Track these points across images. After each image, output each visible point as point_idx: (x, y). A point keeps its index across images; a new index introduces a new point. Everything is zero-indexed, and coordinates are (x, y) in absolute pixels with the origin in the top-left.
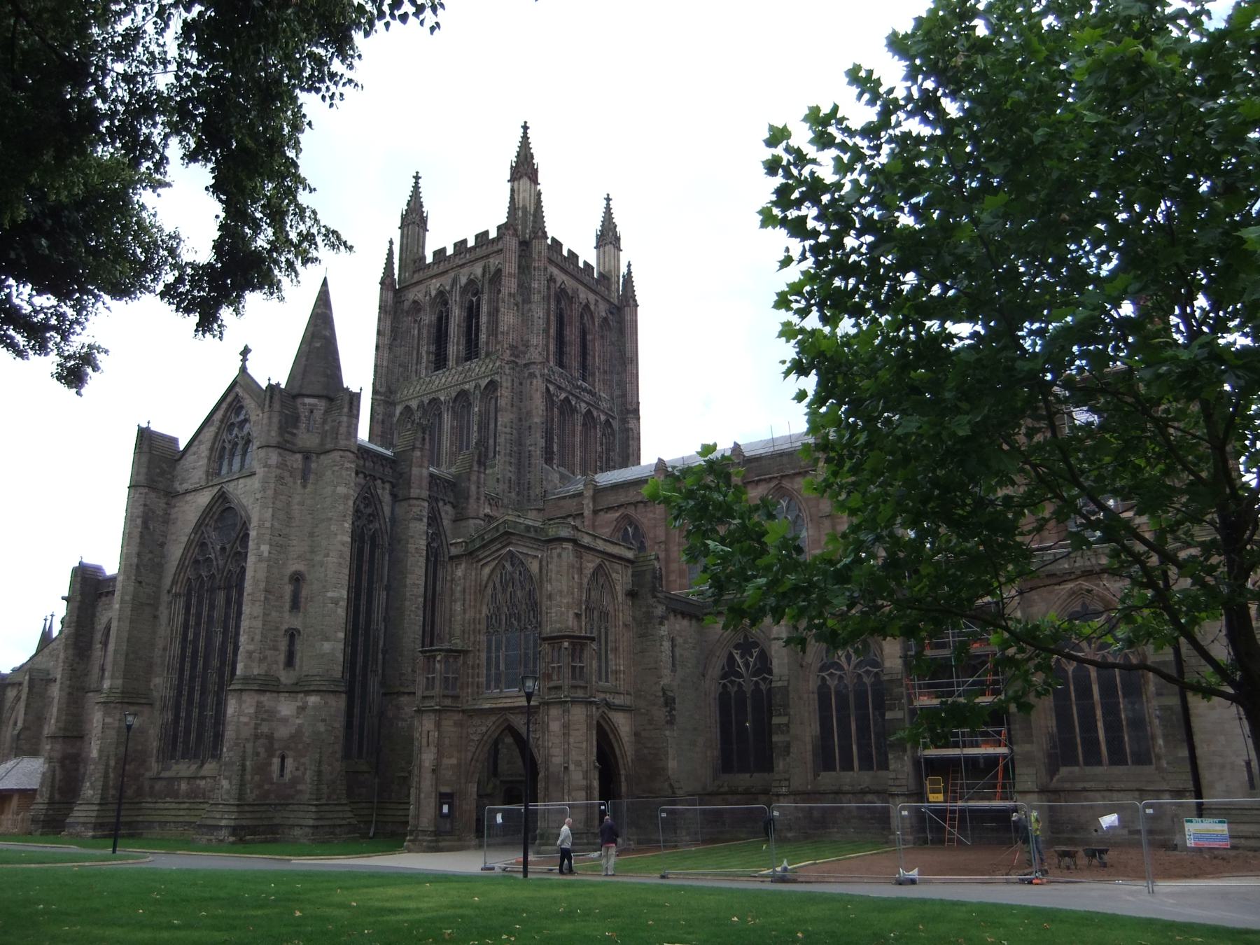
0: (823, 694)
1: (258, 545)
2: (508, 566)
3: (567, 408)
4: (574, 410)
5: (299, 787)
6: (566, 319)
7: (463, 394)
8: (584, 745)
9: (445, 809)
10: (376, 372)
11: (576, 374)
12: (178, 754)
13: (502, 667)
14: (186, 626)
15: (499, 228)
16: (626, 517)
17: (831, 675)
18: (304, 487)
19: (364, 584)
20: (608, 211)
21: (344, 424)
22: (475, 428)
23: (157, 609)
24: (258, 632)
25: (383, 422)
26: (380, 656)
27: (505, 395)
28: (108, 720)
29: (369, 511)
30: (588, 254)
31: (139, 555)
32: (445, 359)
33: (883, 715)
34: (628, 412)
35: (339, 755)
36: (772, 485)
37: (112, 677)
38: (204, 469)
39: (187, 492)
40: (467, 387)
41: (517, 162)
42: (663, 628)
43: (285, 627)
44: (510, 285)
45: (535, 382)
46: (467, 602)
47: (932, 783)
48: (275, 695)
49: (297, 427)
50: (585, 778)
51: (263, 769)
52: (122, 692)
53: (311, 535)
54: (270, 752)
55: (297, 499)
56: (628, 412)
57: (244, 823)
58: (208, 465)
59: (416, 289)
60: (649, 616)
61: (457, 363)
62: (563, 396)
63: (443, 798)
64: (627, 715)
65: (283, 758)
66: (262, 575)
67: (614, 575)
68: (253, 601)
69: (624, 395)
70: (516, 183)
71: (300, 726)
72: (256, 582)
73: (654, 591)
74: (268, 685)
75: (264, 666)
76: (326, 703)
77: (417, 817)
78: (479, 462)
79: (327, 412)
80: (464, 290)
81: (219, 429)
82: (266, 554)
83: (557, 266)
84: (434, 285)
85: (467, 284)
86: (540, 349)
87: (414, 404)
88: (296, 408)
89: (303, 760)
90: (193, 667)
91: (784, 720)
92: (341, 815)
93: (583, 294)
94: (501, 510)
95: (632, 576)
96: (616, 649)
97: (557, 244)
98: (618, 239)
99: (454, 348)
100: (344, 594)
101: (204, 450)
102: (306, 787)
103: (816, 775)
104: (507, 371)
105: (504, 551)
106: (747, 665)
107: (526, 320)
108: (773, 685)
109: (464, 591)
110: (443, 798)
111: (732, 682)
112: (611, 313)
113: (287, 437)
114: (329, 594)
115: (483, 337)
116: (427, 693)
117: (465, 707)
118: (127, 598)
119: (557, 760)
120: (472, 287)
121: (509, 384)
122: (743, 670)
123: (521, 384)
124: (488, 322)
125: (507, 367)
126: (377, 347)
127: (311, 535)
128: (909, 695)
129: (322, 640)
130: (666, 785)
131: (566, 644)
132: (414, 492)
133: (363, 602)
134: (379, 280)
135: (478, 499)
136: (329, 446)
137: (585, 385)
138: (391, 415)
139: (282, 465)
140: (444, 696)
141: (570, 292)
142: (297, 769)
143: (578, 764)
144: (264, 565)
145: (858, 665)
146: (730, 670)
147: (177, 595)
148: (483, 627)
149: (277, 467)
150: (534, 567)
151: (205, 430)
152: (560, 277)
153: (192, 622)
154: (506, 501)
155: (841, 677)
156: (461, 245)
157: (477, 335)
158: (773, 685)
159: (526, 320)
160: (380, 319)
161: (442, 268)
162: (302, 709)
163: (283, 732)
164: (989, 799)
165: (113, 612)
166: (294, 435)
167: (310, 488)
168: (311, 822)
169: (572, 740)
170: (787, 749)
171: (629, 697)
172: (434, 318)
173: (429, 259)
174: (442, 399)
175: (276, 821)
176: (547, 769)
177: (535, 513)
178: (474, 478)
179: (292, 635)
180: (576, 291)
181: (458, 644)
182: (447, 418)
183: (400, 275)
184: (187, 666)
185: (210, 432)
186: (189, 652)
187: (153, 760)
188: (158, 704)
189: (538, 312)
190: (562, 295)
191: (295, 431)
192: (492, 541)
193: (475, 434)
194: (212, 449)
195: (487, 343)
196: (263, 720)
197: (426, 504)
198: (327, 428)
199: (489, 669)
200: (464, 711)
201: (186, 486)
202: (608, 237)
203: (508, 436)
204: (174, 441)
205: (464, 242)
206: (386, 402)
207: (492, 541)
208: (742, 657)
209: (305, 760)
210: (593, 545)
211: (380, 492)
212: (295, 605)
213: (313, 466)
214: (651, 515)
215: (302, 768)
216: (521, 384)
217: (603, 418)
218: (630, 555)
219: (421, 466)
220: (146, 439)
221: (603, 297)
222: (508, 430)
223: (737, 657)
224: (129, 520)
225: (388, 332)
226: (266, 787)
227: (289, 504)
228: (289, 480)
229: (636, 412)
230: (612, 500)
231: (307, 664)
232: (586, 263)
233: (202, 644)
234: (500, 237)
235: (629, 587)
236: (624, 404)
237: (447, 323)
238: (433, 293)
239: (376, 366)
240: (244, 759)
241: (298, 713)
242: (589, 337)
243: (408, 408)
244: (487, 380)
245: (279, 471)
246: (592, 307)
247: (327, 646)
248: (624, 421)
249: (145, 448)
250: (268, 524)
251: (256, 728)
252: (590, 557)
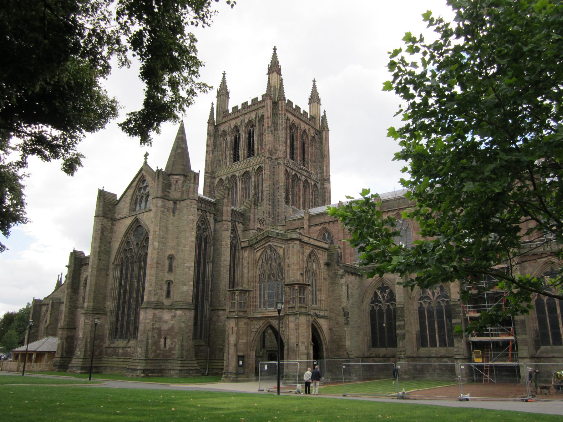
0: (421, 312)
1: (153, 242)
2: (269, 251)
3: (296, 179)
4: (299, 179)
5: (173, 352)
6: (295, 138)
7: (247, 173)
8: (306, 334)
9: (241, 363)
10: (206, 163)
11: (300, 163)
12: (118, 336)
13: (266, 298)
14: (121, 279)
15: (263, 96)
16: (324, 228)
17: (425, 302)
18: (174, 216)
19: (202, 260)
20: (314, 87)
21: (192, 187)
22: (253, 188)
23: (108, 271)
24: (154, 281)
25: (210, 186)
26: (210, 293)
27: (266, 173)
28: (87, 321)
29: (204, 227)
30: (305, 107)
31: (100, 247)
32: (238, 157)
33: (451, 321)
34: (325, 180)
35: (191, 338)
36: (395, 213)
37: (88, 302)
38: (128, 208)
39: (121, 219)
40: (248, 169)
41: (271, 66)
42: (342, 280)
43: (166, 279)
44: (268, 122)
45: (280, 166)
46: (250, 268)
47: (476, 353)
48: (161, 310)
49: (170, 188)
50: (307, 349)
51: (156, 343)
52: (93, 309)
53: (177, 238)
54: (160, 336)
55: (171, 221)
56: (325, 180)
57: (148, 368)
58: (130, 206)
59: (224, 125)
60: (336, 274)
61: (244, 159)
62: (294, 173)
63: (240, 358)
64: (326, 320)
65: (165, 339)
66: (155, 256)
67: (319, 256)
68: (151, 268)
69: (323, 172)
70: (271, 75)
71: (173, 324)
72: (152, 260)
73: (338, 262)
74: (158, 306)
75: (157, 297)
76: (185, 314)
77: (228, 366)
78: (255, 204)
79: (184, 182)
80: (247, 125)
81: (135, 190)
82: (157, 246)
83: (290, 113)
84: (233, 123)
85: (248, 122)
86: (282, 152)
87: (224, 178)
88: (170, 180)
89: (175, 340)
90: (124, 298)
91: (402, 323)
92: (192, 365)
93: (303, 126)
94: (265, 226)
95: (328, 256)
96: (320, 290)
97: (290, 103)
98: (319, 100)
99: (242, 152)
100: (193, 264)
101: (128, 199)
102: (176, 352)
103: (418, 349)
104: (267, 162)
105: (267, 245)
106: (383, 297)
107: (276, 138)
108: (397, 306)
109: (248, 263)
110: (240, 358)
111: (376, 305)
112: (316, 134)
113: (166, 193)
114: (186, 265)
115: (256, 147)
116: (232, 310)
117: (249, 316)
118: (95, 266)
119: (293, 341)
120: (251, 124)
121: (268, 168)
122: (382, 300)
123: (274, 168)
124: (258, 140)
125: (267, 160)
126: (207, 152)
127: (177, 238)
128: (464, 312)
129: (183, 285)
130: (345, 353)
131: (296, 287)
132: (225, 218)
133: (202, 268)
134: (207, 121)
135: (254, 221)
136: (185, 197)
137: (304, 168)
138: (214, 183)
139: (164, 206)
140: (239, 311)
141: (296, 125)
142: (172, 344)
143: (303, 342)
144: (156, 251)
145: (438, 297)
146: (375, 300)
147: (117, 265)
148: (257, 279)
149: (161, 207)
150: (281, 252)
151: (129, 191)
152: (292, 118)
153: (124, 277)
154: (267, 222)
155: (430, 303)
156: (245, 105)
157: (253, 146)
158: (397, 306)
159: (276, 138)
160: (208, 139)
161: (236, 115)
162: (174, 316)
163: (165, 327)
164: (505, 361)
165: (88, 273)
166: (169, 192)
167: (176, 216)
168: (179, 368)
169: (300, 332)
170: (404, 336)
171: (326, 312)
172: (233, 138)
173: (230, 111)
174: (237, 175)
175: (163, 367)
176: (288, 345)
177: (281, 227)
178: (252, 211)
179: (169, 283)
180: (299, 125)
181: (246, 287)
182: (239, 184)
183: (217, 119)
184: (122, 297)
185: (131, 192)
186: (122, 291)
187: (107, 339)
188: (109, 314)
189: (282, 134)
190: (293, 126)
192: (261, 240)
193: (253, 191)
194: (132, 199)
195: (258, 149)
196: (156, 321)
197: (230, 223)
198: (184, 189)
199: (260, 299)
200: (249, 318)
201: (120, 216)
202: (314, 99)
203: (268, 192)
204: (115, 195)
205: (247, 103)
206: (211, 177)
207: (261, 240)
208: (381, 293)
209: (176, 340)
210: (308, 242)
211: (208, 218)
212: (170, 269)
213: (178, 206)
214: (336, 228)
215: (174, 343)
216: (274, 168)
217: (313, 183)
218: (326, 246)
219: (228, 206)
220: (103, 196)
221: (312, 127)
222: (268, 189)
223: (379, 294)
224: (95, 231)
225: (211, 145)
226: (158, 352)
227: (167, 224)
228: (166, 212)
229: (328, 180)
230: (318, 221)
231: (176, 296)
232: (304, 111)
233: (128, 287)
234: (263, 101)
235: (326, 261)
236: (323, 176)
237: (239, 140)
238: (232, 127)
239: (206, 161)
240: (148, 339)
241: (172, 319)
242: (306, 146)
243: (221, 179)
244: (258, 167)
245: (162, 209)
246: (307, 132)
247: (185, 288)
248: (323, 184)
249: (102, 199)
250: (157, 233)
251: (153, 325)
252: (307, 247)
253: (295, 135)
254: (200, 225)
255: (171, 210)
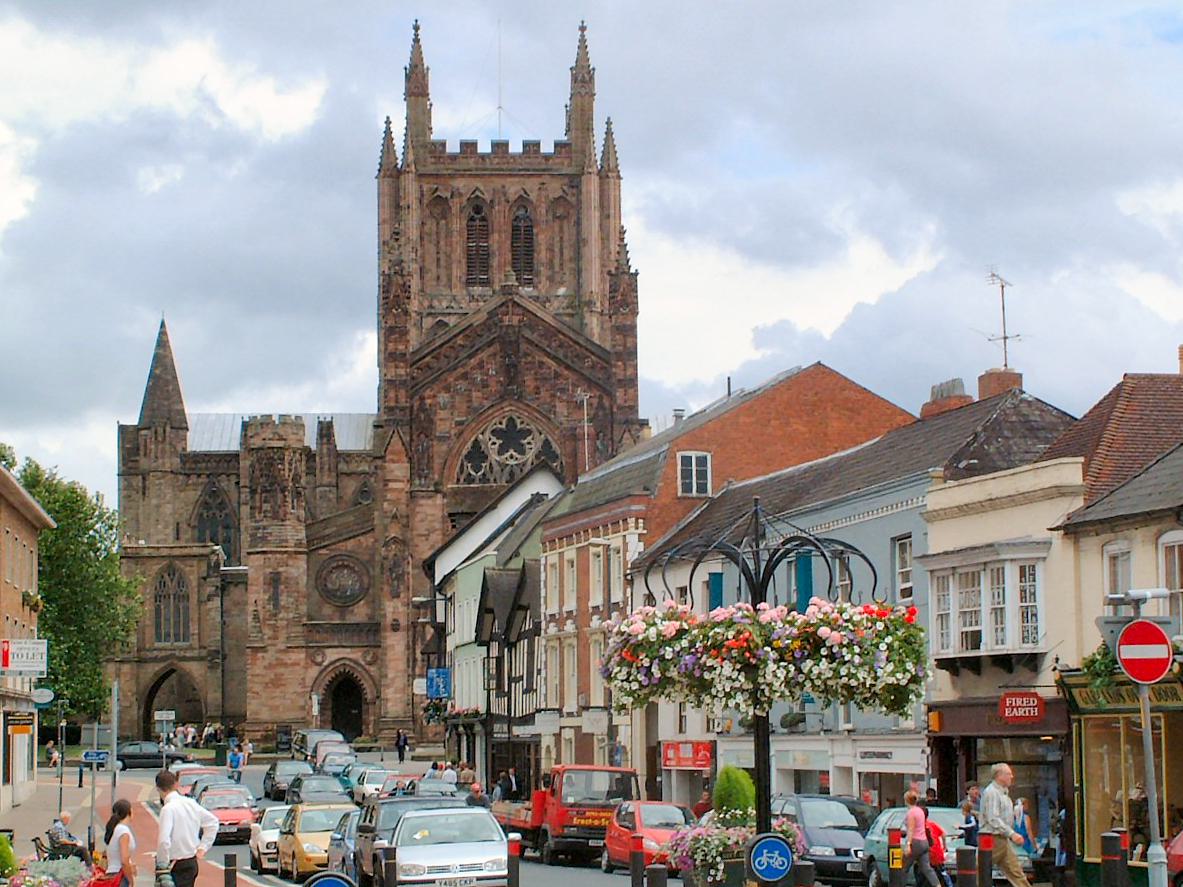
20: (583, 45)
49: (138, 455)
135: (322, 468)
141: (487, 197)
166: (137, 461)
191: (138, 458)
227: (137, 514)
228: (134, 496)
245: (126, 492)
254: (210, 501)
255: (141, 493)
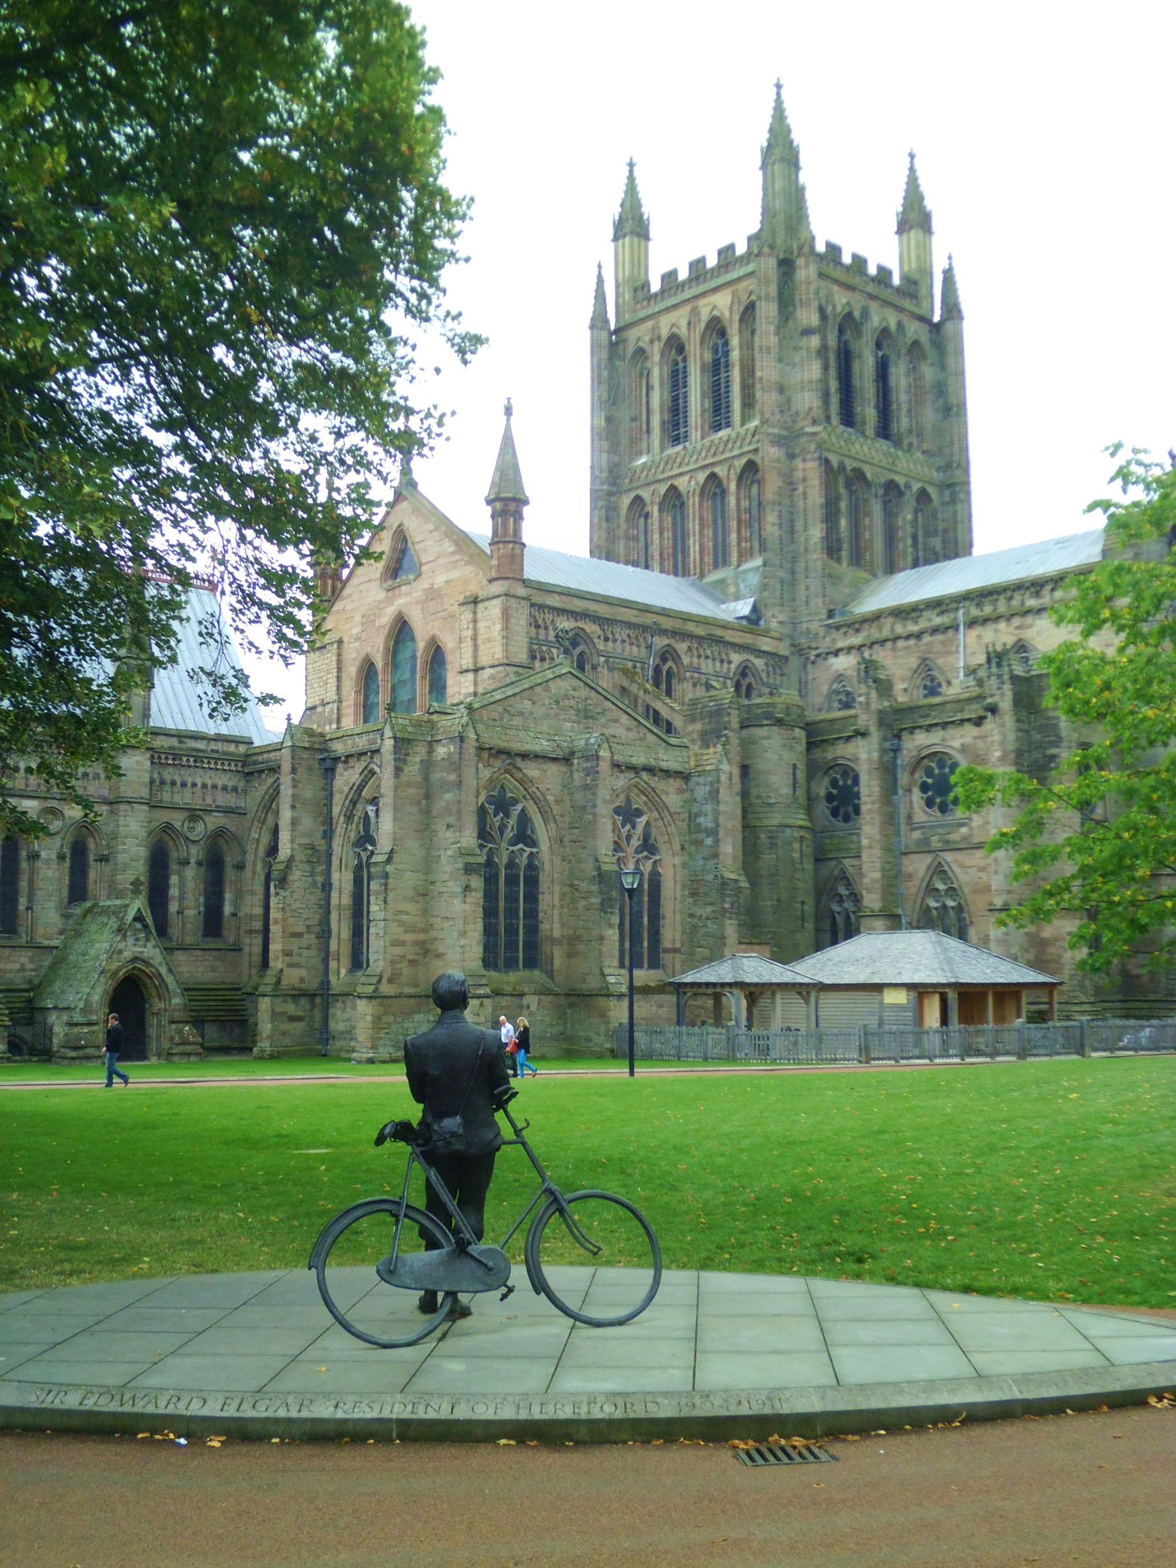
87: (645, 494)
97: (834, 250)
134: (588, 322)
152: (841, 299)
156: (697, 265)
173: (655, 286)
205: (702, 261)
232: (881, 269)
243: (638, 498)
244: (744, 461)
253: (854, 346)
